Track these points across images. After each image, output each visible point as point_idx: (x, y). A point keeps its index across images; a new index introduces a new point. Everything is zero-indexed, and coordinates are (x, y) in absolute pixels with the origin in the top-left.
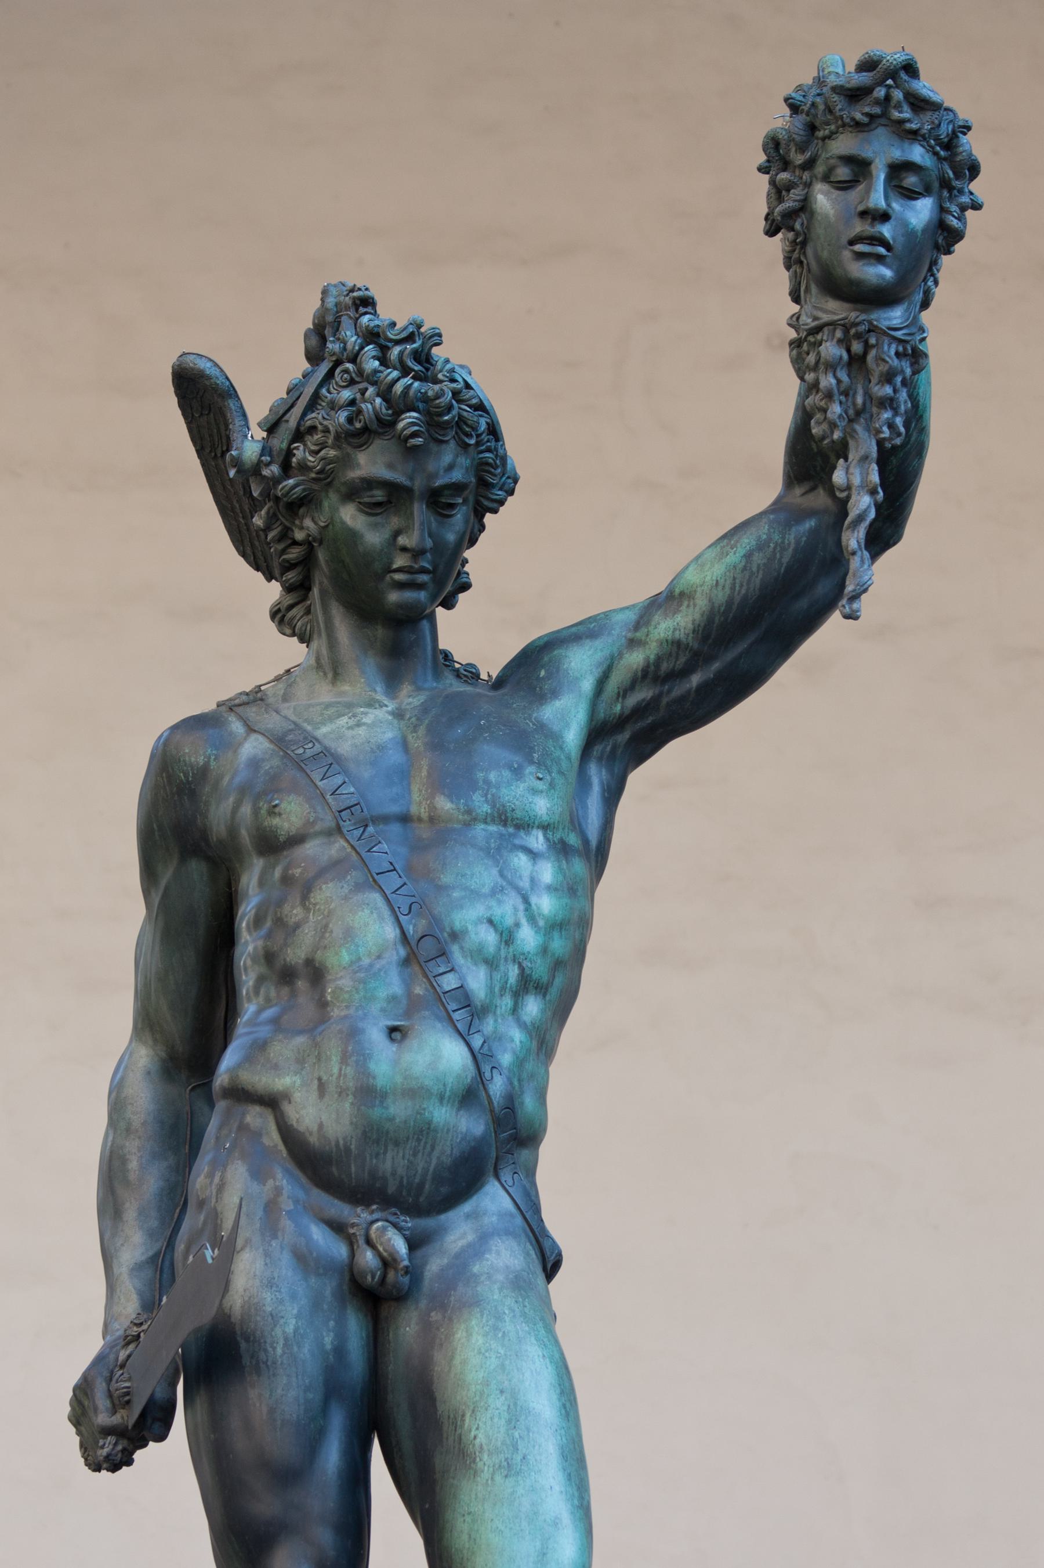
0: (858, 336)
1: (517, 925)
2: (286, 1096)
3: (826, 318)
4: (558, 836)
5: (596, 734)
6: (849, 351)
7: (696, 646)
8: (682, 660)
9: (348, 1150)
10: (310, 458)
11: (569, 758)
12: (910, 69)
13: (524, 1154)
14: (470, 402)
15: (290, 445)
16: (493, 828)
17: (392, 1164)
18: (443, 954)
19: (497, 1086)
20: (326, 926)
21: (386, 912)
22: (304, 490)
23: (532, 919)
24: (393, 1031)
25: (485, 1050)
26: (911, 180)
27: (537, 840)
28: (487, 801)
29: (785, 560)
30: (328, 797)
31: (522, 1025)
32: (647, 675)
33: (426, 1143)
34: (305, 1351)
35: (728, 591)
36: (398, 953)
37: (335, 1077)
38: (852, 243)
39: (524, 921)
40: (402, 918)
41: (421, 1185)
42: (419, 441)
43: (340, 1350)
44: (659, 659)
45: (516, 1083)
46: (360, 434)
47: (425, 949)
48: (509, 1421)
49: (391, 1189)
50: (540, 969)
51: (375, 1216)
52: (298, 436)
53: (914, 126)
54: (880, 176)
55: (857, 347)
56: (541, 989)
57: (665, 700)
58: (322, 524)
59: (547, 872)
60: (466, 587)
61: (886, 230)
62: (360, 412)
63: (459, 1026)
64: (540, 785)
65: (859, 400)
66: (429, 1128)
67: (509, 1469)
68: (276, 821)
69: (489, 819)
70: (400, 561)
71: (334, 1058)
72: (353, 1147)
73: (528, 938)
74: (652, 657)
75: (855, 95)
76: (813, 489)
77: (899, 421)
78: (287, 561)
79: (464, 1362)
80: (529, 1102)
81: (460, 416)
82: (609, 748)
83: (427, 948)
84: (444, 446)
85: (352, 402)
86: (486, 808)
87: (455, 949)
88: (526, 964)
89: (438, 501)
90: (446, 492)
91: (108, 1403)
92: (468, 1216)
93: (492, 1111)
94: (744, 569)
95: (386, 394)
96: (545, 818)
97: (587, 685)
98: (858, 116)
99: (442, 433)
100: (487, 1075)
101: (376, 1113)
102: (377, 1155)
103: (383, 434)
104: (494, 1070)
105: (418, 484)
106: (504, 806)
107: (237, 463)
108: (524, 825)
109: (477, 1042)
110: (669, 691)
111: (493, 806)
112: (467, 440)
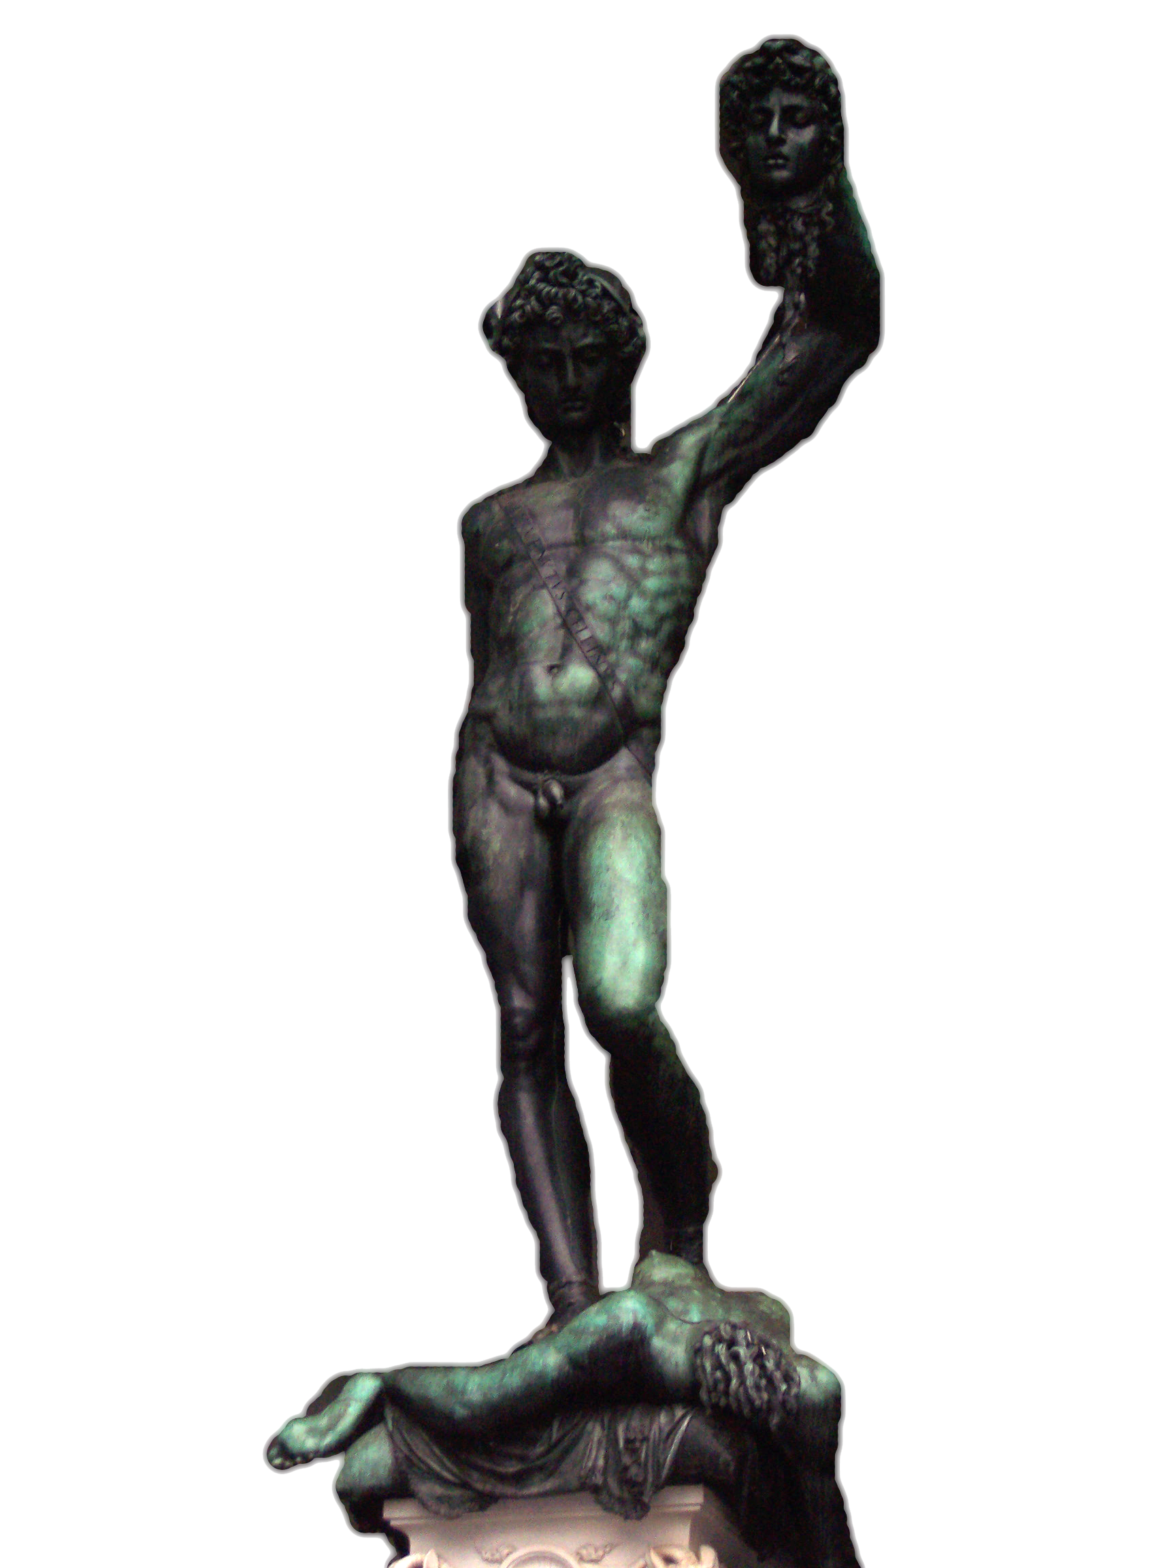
1: (629, 597)
4: (664, 542)
6: (777, 226)
13: (646, 733)
16: (618, 543)
23: (643, 594)
24: (551, 669)
26: (800, 115)
27: (646, 547)
34: (507, 859)
38: (767, 158)
41: (571, 758)
43: (529, 858)
50: (648, 622)
56: (652, 633)
59: (654, 564)
61: (785, 149)
73: (637, 604)
74: (732, 432)
77: (811, 264)
80: (643, 702)
85: (522, 306)
86: (613, 531)
95: (539, 300)
96: (653, 533)
101: (541, 715)
105: (566, 351)
108: (636, 538)
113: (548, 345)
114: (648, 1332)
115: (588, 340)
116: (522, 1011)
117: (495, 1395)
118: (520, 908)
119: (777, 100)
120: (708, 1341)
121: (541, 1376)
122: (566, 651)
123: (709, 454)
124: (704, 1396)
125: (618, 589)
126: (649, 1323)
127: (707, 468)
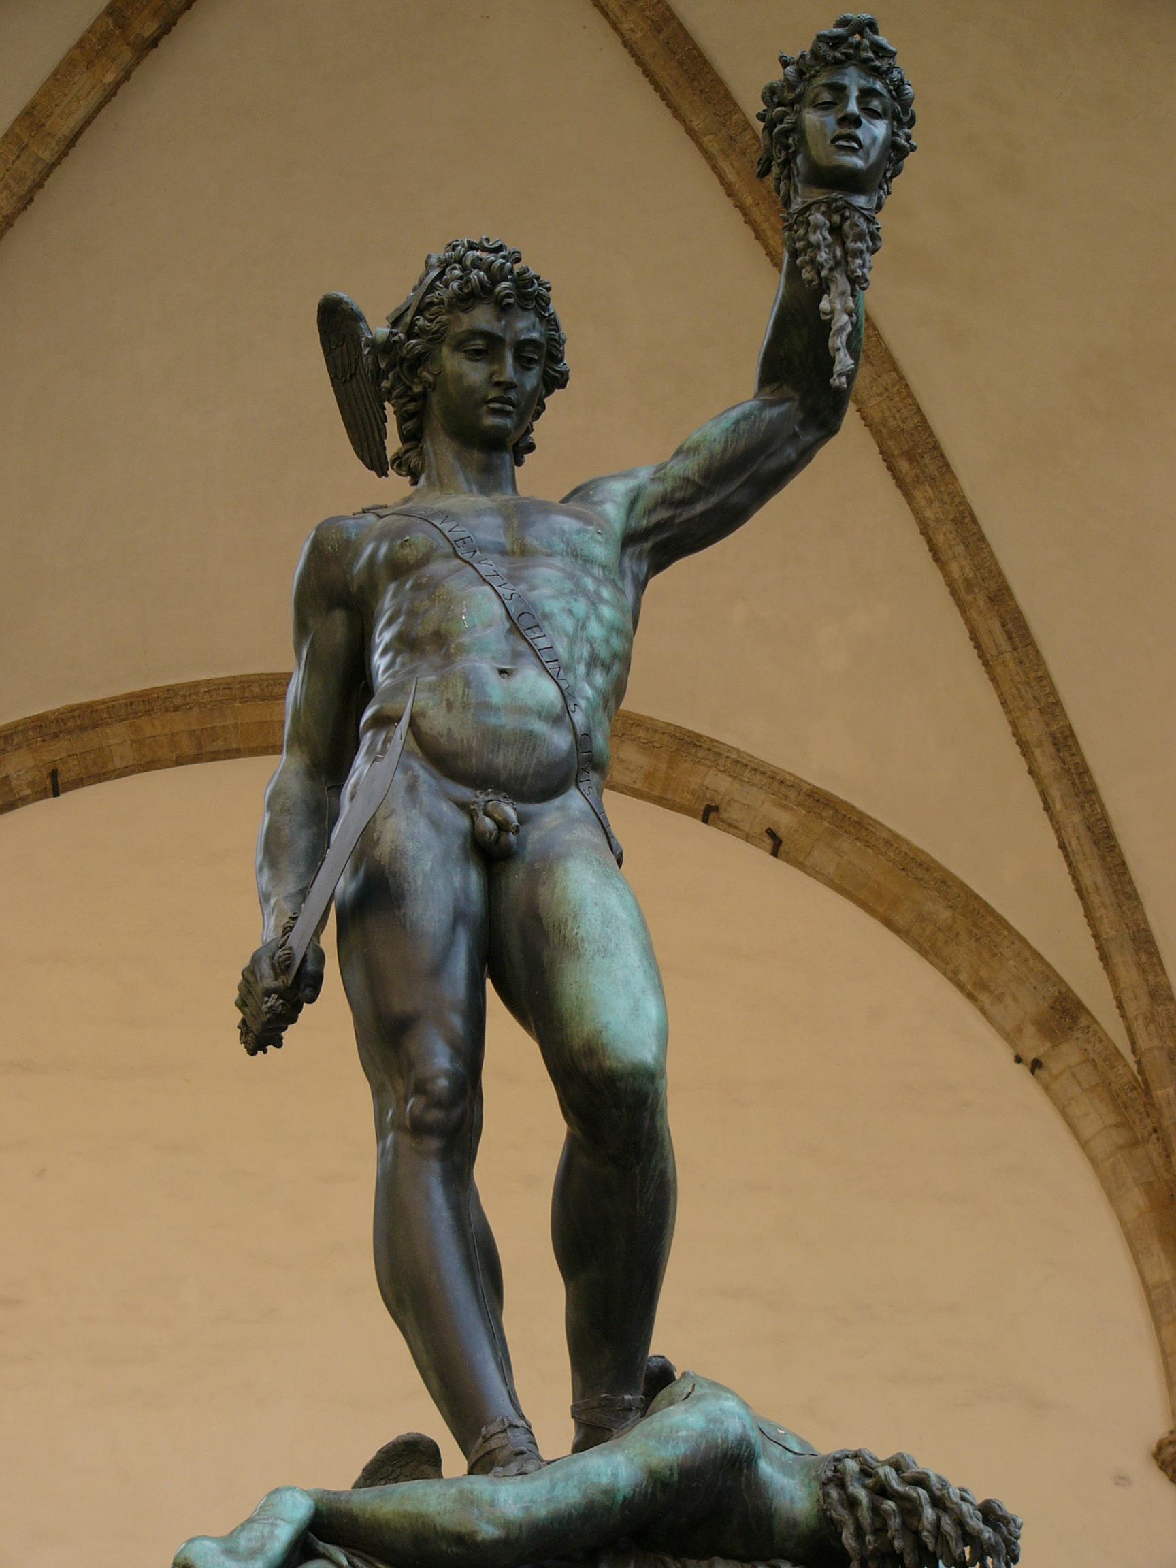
0: (837, 210)
1: (588, 618)
3: (810, 201)
4: (612, 577)
5: (630, 539)
7: (700, 482)
8: (690, 491)
9: (470, 748)
12: (872, 25)
17: (504, 760)
19: (579, 718)
20: (448, 609)
21: (495, 597)
23: (600, 619)
26: (875, 104)
27: (597, 571)
29: (763, 428)
31: (593, 687)
32: (665, 501)
35: (722, 445)
39: (593, 617)
41: (525, 776)
42: (511, 300)
44: (673, 491)
46: (468, 298)
47: (522, 624)
48: (603, 923)
49: (503, 777)
50: (604, 653)
51: (490, 797)
53: (877, 63)
54: (854, 93)
55: (836, 218)
56: (607, 668)
59: (606, 593)
60: (531, 448)
62: (469, 281)
64: (599, 538)
65: (839, 253)
67: (605, 953)
68: (406, 551)
70: (493, 394)
74: (669, 489)
75: (835, 42)
76: (780, 387)
78: (406, 412)
79: (565, 888)
80: (600, 740)
83: (525, 622)
84: (526, 313)
85: (461, 278)
86: (562, 546)
87: (546, 624)
88: (595, 646)
89: (525, 353)
90: (528, 349)
91: (272, 973)
92: (558, 808)
93: (575, 734)
94: (734, 431)
97: (623, 501)
98: (838, 55)
100: (572, 707)
101: (492, 721)
102: (492, 751)
103: (484, 299)
105: (508, 338)
107: (372, 344)
109: (564, 686)
110: (680, 515)
114: (758, 1448)
115: (535, 335)
116: (446, 1074)
117: (542, 1512)
118: (450, 945)
119: (853, 81)
120: (852, 1466)
121: (609, 1492)
122: (516, 656)
123: (640, 507)
124: (848, 1538)
125: (581, 607)
126: (754, 1436)
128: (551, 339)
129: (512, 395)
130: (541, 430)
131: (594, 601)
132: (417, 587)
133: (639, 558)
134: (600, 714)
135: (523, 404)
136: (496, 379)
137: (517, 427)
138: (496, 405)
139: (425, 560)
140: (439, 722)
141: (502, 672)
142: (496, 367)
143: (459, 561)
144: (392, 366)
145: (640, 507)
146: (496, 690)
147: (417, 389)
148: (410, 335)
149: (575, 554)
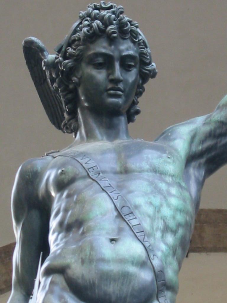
1: (161, 205)
2: (68, 267)
4: (178, 181)
9: (94, 284)
10: (74, 51)
11: (181, 157)
14: (135, 25)
15: (66, 48)
16: (150, 174)
18: (132, 213)
19: (156, 262)
20: (84, 207)
22: (72, 64)
23: (169, 205)
25: (151, 248)
27: (169, 179)
28: (148, 164)
30: (84, 165)
31: (166, 244)
32: (211, 135)
33: (127, 281)
36: (113, 213)
37: (88, 256)
39: (165, 205)
40: (114, 200)
41: (125, 298)
42: (115, 35)
44: (215, 129)
45: (164, 263)
50: (172, 224)
52: (70, 44)
57: (219, 145)
58: (79, 77)
59: (174, 190)
60: (138, 112)
62: (92, 27)
63: (139, 238)
64: (169, 160)
66: (128, 274)
68: (63, 176)
69: (149, 171)
70: (110, 86)
71: (87, 249)
72: (96, 282)
73: (166, 212)
81: (131, 30)
82: (197, 165)
83: (125, 211)
84: (125, 41)
85: (88, 25)
87: (136, 212)
89: (126, 63)
93: (154, 271)
99: (124, 35)
100: (152, 257)
104: (155, 256)
105: (116, 54)
106: (155, 166)
109: (147, 245)
110: (220, 141)
111: (151, 166)
112: (135, 40)
113: (103, 51)
115: (131, 52)
122: (120, 230)
127: (194, 149)
128: (142, 54)
129: (121, 86)
130: (142, 103)
131: (166, 196)
132: (69, 196)
133: (199, 167)
134: (170, 259)
135: (127, 90)
136: (111, 77)
137: (125, 102)
138: (112, 92)
139: (72, 180)
140: (77, 270)
141: (112, 240)
142: (110, 71)
143: (90, 180)
144: (57, 75)
145: (197, 140)
146: (107, 250)
147: (71, 86)
148: (65, 58)
149: (155, 170)
